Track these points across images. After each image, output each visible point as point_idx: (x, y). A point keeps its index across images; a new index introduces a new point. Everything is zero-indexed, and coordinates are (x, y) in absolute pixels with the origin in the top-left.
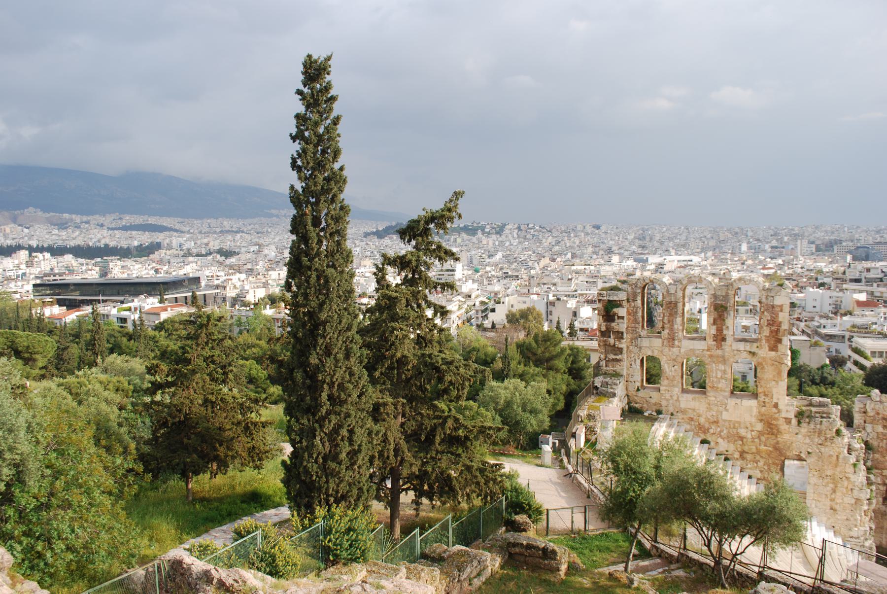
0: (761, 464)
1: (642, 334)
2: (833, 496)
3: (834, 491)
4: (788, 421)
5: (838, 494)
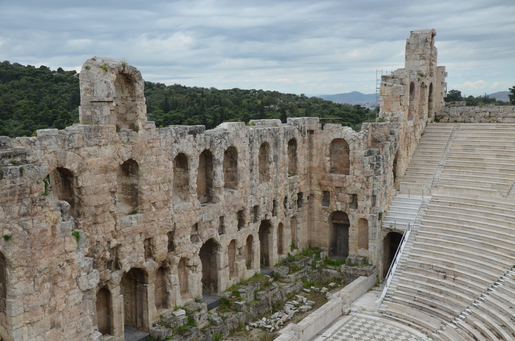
2: (53, 303)
5: (60, 295)
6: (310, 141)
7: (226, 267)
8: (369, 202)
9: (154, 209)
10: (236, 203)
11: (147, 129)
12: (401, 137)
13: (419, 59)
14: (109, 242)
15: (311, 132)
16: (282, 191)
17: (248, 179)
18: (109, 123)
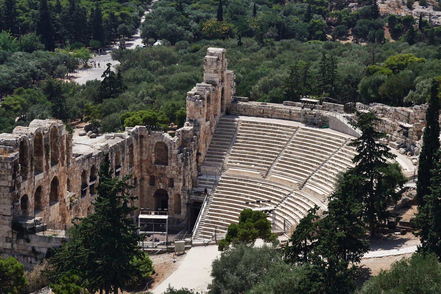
8: (181, 184)
12: (201, 136)
13: (213, 72)
15: (142, 137)
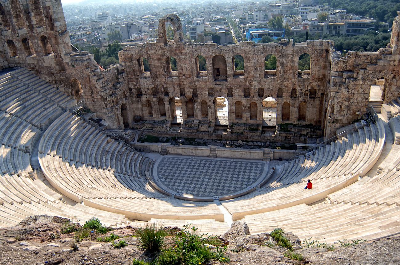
0: (63, 85)
1: (4, 29)
2: (92, 96)
3: (92, 93)
4: (67, 63)
5: (94, 94)
6: (327, 56)
7: (232, 112)
9: (184, 77)
10: (241, 84)
11: (179, 45)
14: (163, 85)
16: (289, 85)
17: (253, 73)
18: (159, 42)
